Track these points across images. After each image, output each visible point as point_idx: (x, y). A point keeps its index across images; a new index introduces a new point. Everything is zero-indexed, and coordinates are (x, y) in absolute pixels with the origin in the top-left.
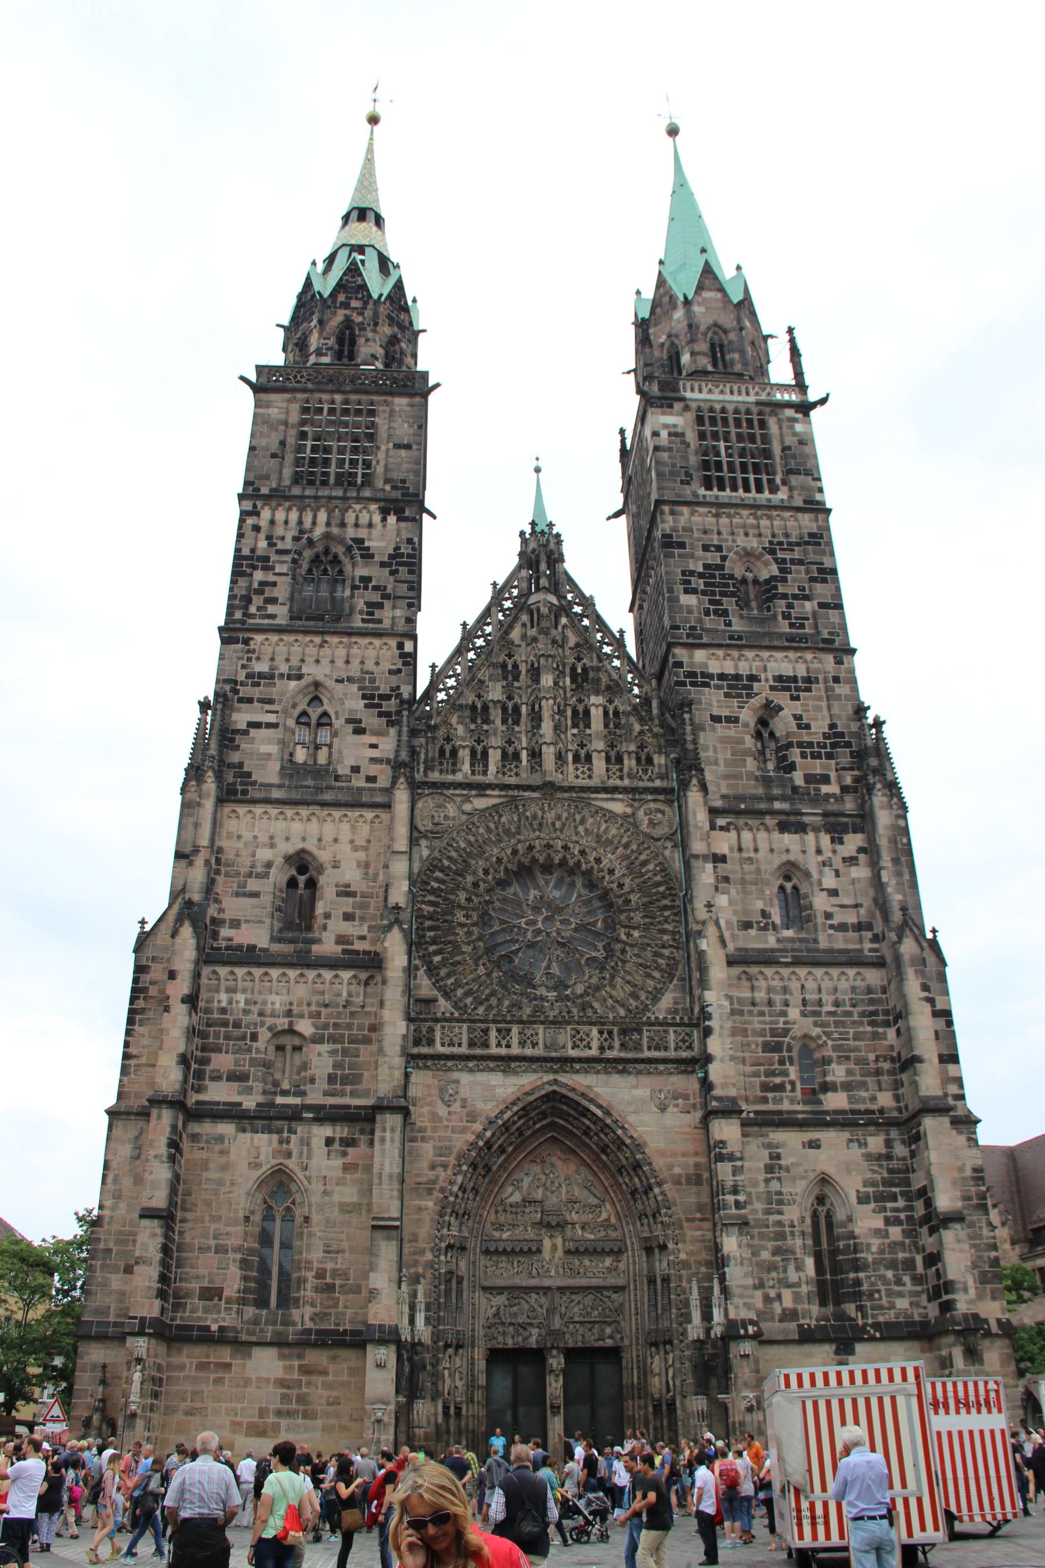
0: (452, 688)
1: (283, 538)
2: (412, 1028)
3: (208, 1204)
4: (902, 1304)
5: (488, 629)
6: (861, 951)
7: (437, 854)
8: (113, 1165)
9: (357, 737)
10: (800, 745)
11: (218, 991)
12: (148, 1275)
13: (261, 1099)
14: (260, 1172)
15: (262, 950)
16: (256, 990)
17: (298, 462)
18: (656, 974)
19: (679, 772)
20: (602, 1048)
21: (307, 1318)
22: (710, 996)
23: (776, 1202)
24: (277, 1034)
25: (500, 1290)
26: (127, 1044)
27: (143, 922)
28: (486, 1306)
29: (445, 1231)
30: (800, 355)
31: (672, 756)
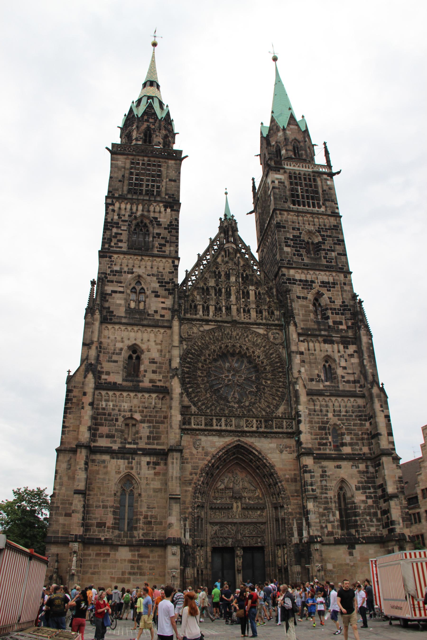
0: (194, 280)
1: (124, 215)
3: (99, 488)
4: (373, 529)
5: (208, 257)
6: (355, 391)
7: (189, 347)
8: (59, 471)
10: (331, 309)
11: (101, 401)
12: (77, 518)
13: (120, 445)
14: (120, 475)
15: (119, 384)
16: (117, 400)
17: (130, 184)
18: (277, 398)
19: (284, 317)
20: (257, 427)
21: (140, 535)
22: (301, 408)
23: (325, 489)
24: (126, 419)
25: (216, 524)
26: (64, 422)
27: (69, 371)
28: (211, 530)
29: (196, 500)
30: (329, 154)
31: (282, 311)
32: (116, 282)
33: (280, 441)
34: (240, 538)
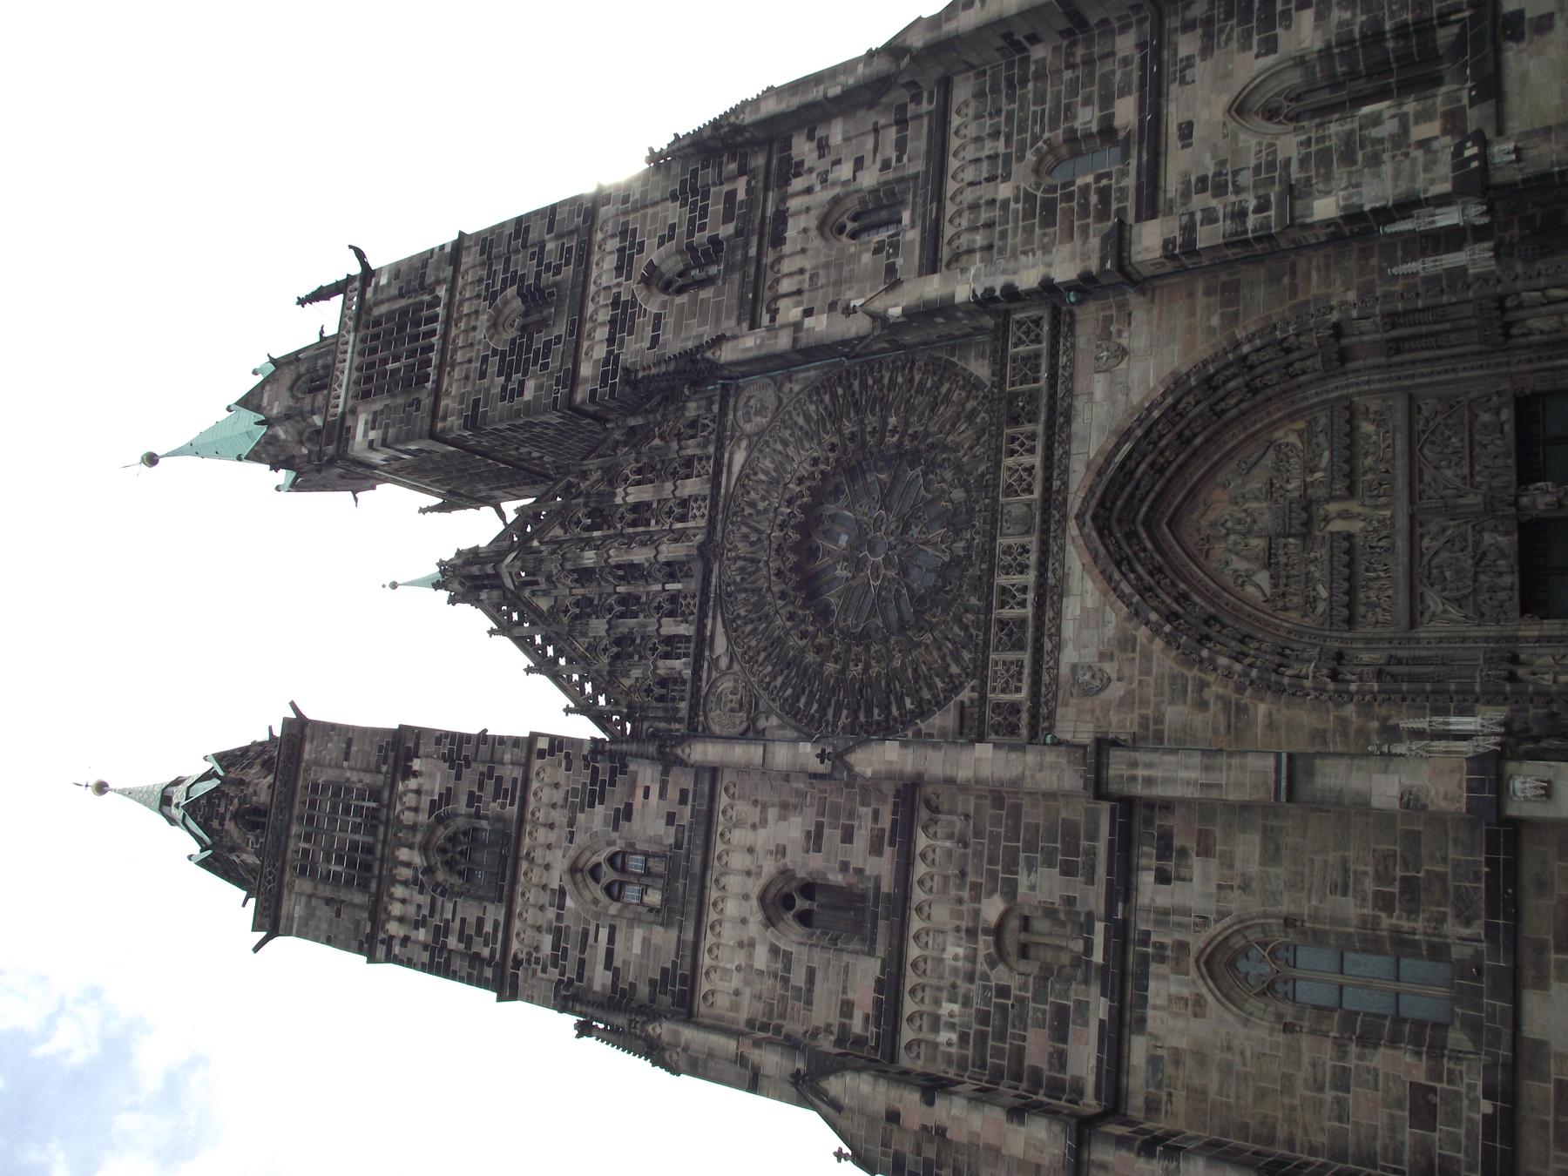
2: (993, 737)
3: (1261, 1095)
6: (930, 113)
9: (636, 815)
10: (691, 234)
11: (936, 1045)
13: (1095, 989)
14: (1210, 998)
17: (349, 883)
18: (944, 389)
21: (1466, 932)
29: (1308, 683)
31: (686, 391)
32: (583, 951)
33: (1084, 362)
34: (1480, 499)
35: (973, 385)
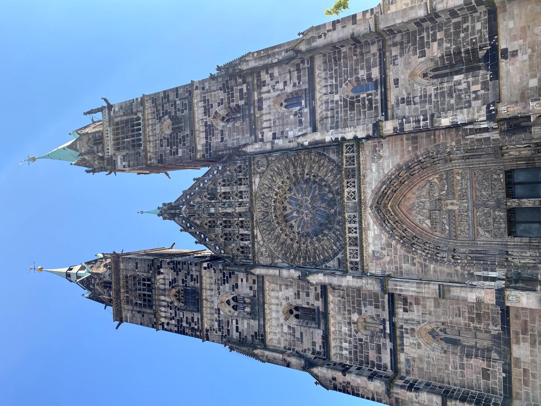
1: (171, 314)
3: (439, 370)
4: (478, 26)
6: (308, 68)
10: (229, 103)
13: (388, 340)
16: (340, 337)
17: (145, 306)
18: (322, 161)
22: (328, 139)
23: (425, 98)
26: (368, 398)
33: (368, 159)
35: (331, 160)
